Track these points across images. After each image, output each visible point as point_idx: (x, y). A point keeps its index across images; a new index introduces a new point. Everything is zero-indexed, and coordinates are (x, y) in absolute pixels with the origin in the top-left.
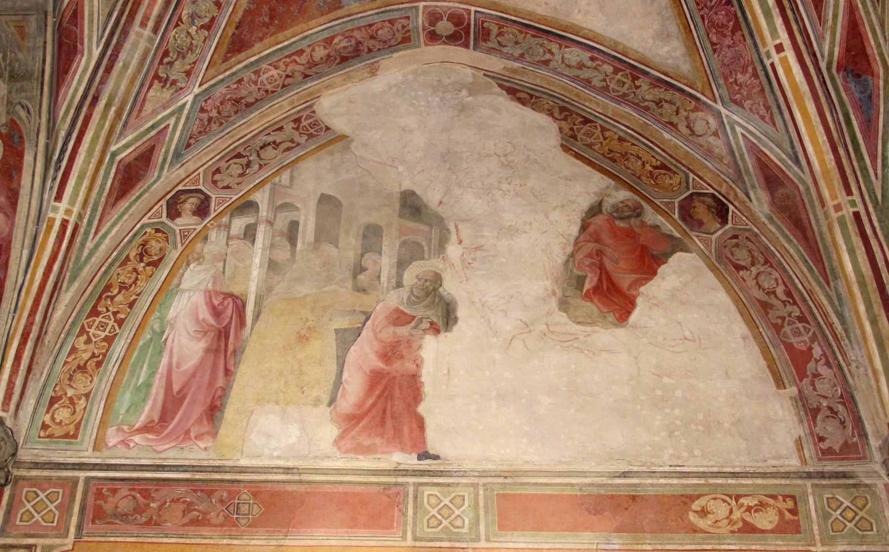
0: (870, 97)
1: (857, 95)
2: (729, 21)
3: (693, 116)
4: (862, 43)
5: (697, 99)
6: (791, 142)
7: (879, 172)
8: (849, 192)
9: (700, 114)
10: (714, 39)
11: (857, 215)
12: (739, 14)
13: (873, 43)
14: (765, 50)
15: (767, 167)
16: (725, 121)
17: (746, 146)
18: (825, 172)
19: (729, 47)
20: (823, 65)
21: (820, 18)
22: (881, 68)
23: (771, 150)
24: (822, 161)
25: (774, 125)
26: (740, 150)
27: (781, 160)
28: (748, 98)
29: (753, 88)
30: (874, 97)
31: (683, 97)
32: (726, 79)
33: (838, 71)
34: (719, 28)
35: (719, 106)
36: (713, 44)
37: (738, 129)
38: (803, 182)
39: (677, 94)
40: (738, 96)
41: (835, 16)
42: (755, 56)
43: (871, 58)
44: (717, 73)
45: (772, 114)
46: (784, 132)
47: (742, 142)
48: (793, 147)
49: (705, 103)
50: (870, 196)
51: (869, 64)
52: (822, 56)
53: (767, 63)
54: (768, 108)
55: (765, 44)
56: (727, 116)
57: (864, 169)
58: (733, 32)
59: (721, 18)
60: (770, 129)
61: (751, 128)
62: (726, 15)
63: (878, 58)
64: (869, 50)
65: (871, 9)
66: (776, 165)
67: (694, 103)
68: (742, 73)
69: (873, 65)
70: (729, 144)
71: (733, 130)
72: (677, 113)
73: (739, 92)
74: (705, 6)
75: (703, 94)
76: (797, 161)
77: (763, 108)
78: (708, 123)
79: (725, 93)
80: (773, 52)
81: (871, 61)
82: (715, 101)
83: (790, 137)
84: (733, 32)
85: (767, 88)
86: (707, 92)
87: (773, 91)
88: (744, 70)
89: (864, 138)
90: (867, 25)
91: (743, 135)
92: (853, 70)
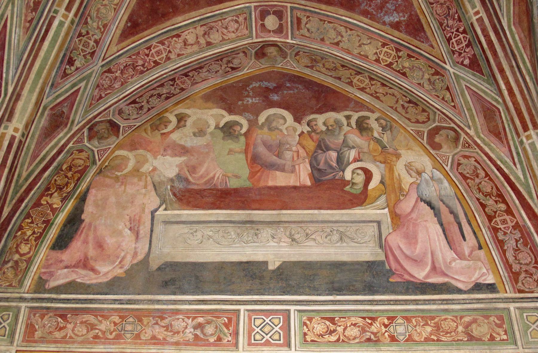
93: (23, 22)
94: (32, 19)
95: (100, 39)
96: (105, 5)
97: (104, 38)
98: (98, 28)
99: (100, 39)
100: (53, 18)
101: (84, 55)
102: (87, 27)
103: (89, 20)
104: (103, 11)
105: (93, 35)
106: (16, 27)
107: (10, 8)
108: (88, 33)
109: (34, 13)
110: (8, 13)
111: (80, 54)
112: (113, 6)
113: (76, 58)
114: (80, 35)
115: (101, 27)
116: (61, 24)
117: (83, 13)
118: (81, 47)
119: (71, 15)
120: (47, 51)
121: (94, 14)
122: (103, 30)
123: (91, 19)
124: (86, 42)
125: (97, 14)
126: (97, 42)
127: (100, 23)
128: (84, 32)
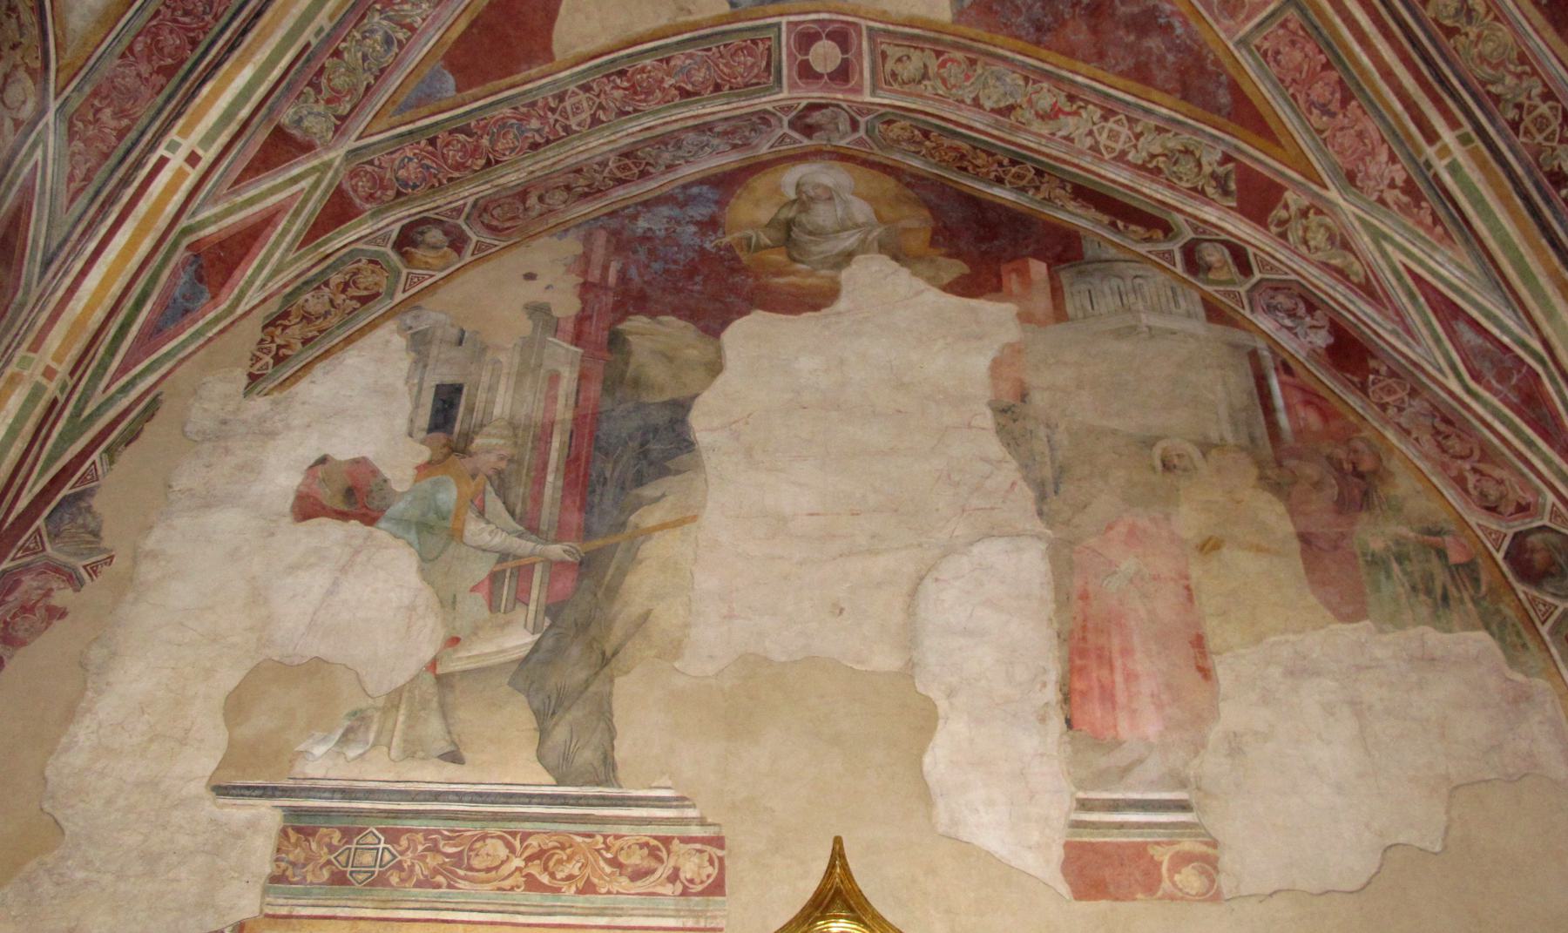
0: (186, 311)
1: (177, 292)
2: (171, 56)
3: (21, 74)
4: (241, 259)
5: (46, 67)
6: (65, 240)
7: (114, 388)
8: (72, 374)
9: (29, 83)
10: (138, 47)
11: (55, 402)
12: (186, 66)
13: (249, 272)
14: (177, 139)
15: (17, 228)
16: (40, 126)
17: (25, 180)
18: (79, 323)
19: (139, 75)
20: (184, 222)
21: (237, 182)
22: (228, 303)
23: (39, 220)
24: (90, 308)
25: (72, 200)
26: (17, 175)
27: (35, 241)
28: (87, 142)
29: (103, 141)
30: (190, 316)
31: (37, 42)
32: (95, 94)
33: (189, 247)
34: (155, 47)
35: (53, 106)
36: (130, 48)
37: (39, 154)
38: (27, 293)
39: (36, 31)
40: (80, 125)
41: (251, 202)
42: (144, 121)
43: (231, 281)
44: (96, 76)
45: (81, 189)
46: (71, 220)
47: (26, 170)
48: (60, 247)
49: (46, 81)
50: (79, 400)
51: (223, 285)
52: (194, 214)
53: (161, 151)
54: (88, 178)
55: (185, 133)
56: (47, 125)
57: (103, 366)
58: (160, 70)
59: (170, 41)
60: (63, 199)
61: (49, 171)
62: (177, 48)
63: (236, 291)
64: (237, 273)
65: (284, 245)
66: (26, 238)
67: (38, 64)
68: (114, 114)
69: (225, 290)
70: (14, 152)
71: (34, 146)
72: (14, 47)
73: (86, 123)
74: (174, 10)
75: (58, 71)
76: (46, 265)
77: (84, 171)
78: (24, 102)
79: (76, 103)
80: (183, 152)
81: (228, 285)
82: (57, 96)
83: (70, 233)
84: (160, 70)
85: (113, 160)
86: (63, 76)
87: (113, 171)
88: (120, 114)
89: (137, 338)
90: (263, 252)
91: (36, 164)
92: (201, 266)
93: (1428, 237)
94: (1433, 214)
95: (1545, 85)
96: (1479, 36)
97: (1548, 74)
98: (1519, 76)
99: (1545, 85)
100: (1436, 176)
101: (1561, 141)
102: (1507, 101)
103: (1492, 89)
104: (1488, 47)
105: (1529, 98)
106: (1431, 257)
107: (1389, 248)
108: (1519, 106)
109: (1424, 204)
110: (1397, 257)
111: (1554, 149)
112: (1486, 21)
113: (1556, 163)
114: (1515, 125)
115: (1520, 69)
116: (1454, 168)
117: (1473, 95)
118: (1539, 138)
119: (1447, 136)
120: (1491, 229)
121: (1485, 72)
122: (1527, 68)
123: (1493, 83)
124: (1534, 121)
125: (1489, 64)
126: (1548, 96)
127: (1512, 67)
128: (1512, 114)
